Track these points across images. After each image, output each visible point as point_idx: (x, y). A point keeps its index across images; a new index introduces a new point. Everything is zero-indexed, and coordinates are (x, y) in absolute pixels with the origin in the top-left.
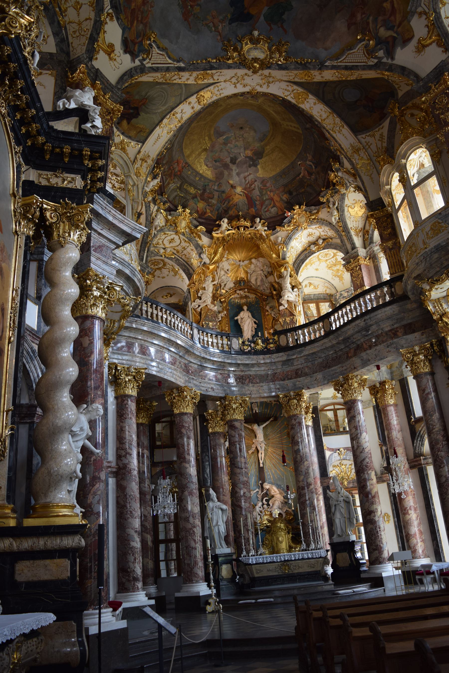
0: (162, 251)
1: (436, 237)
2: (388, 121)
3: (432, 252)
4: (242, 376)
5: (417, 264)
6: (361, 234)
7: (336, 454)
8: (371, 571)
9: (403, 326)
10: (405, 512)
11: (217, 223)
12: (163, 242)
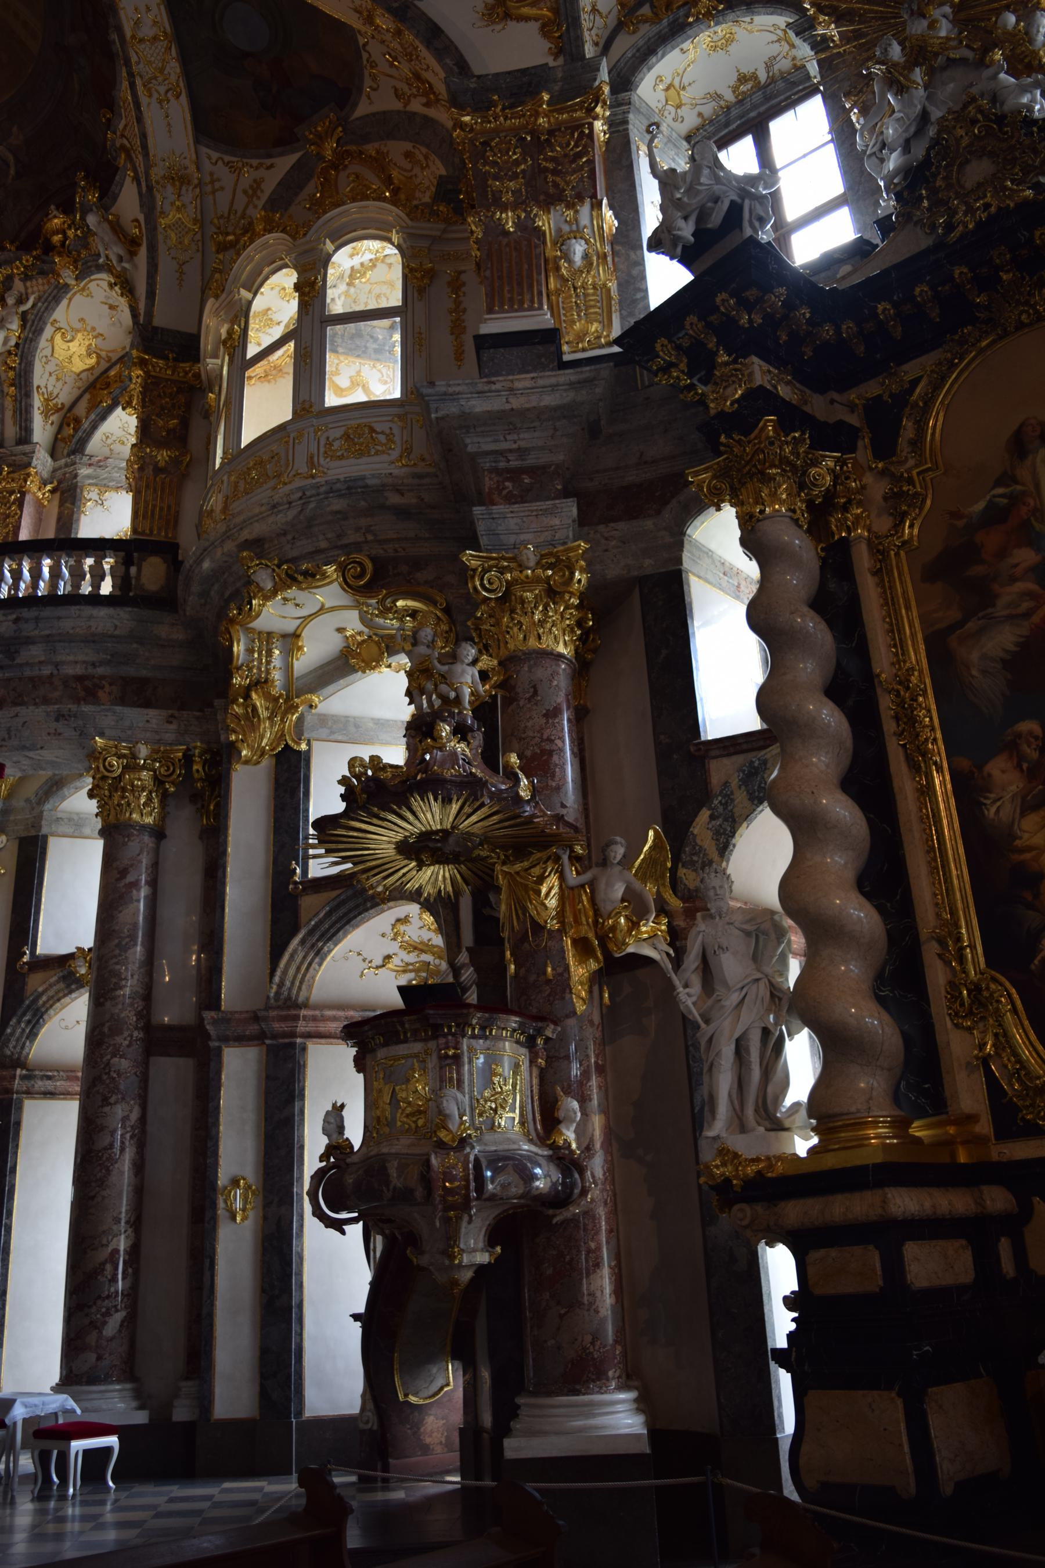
1: (352, 461)
2: (293, 159)
3: (332, 490)
5: (274, 507)
6: (54, 418)
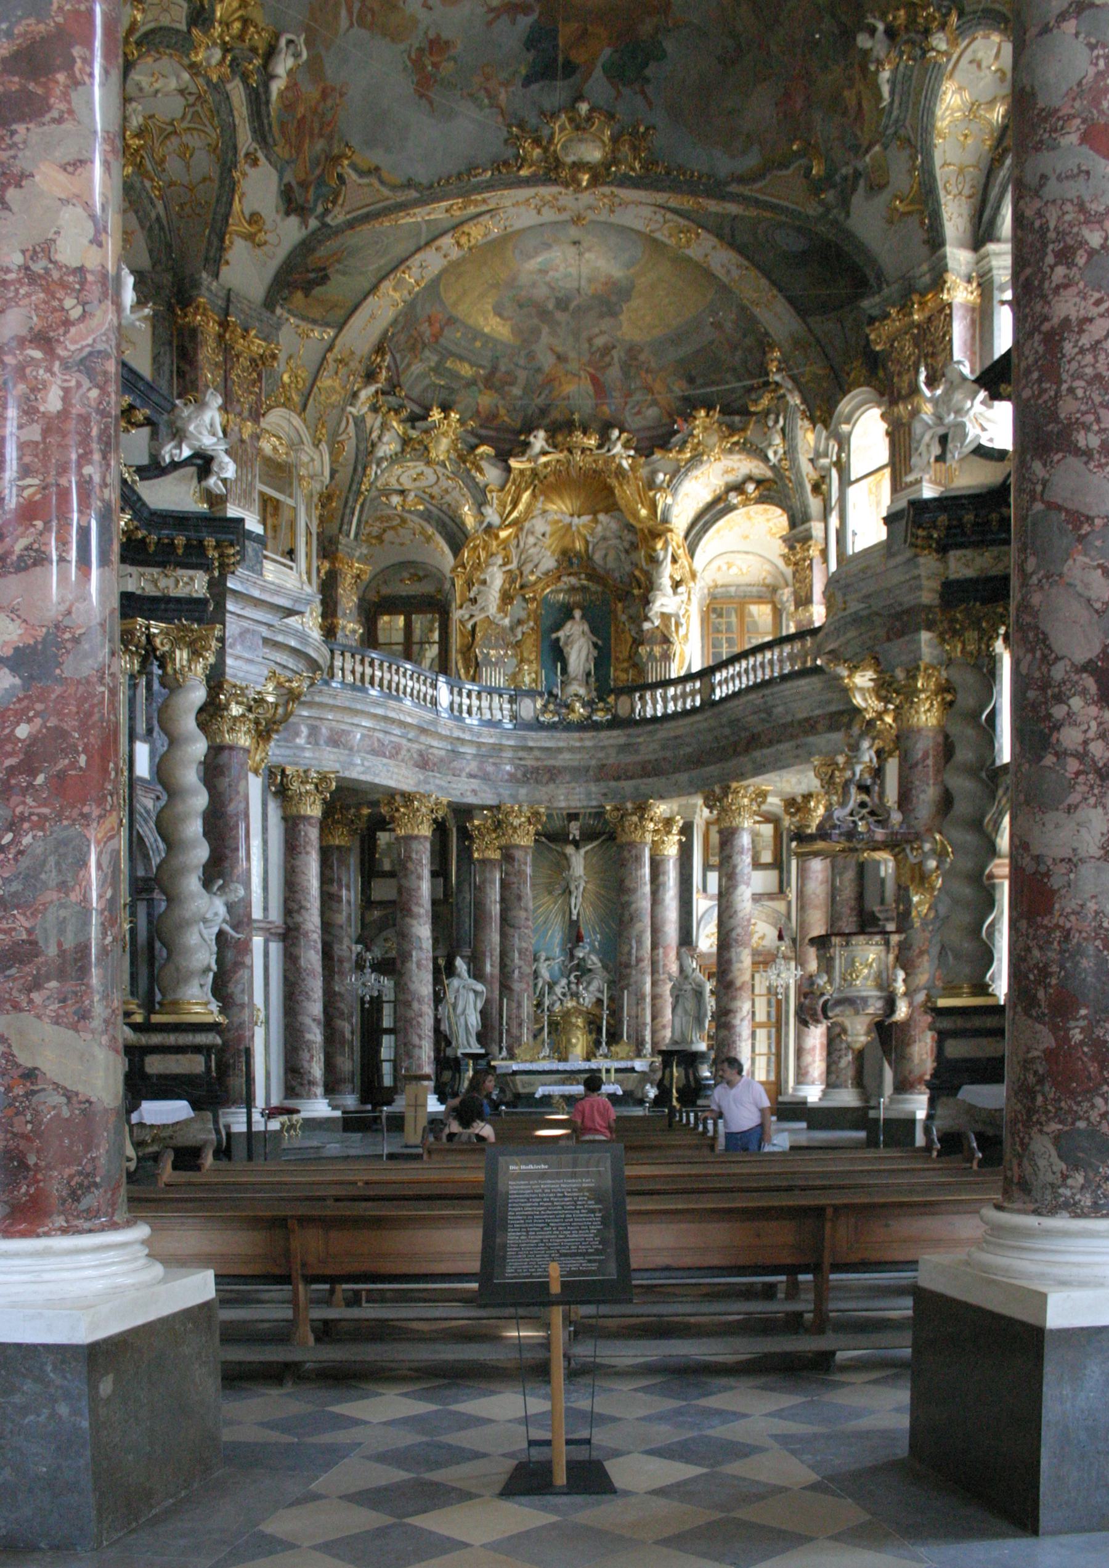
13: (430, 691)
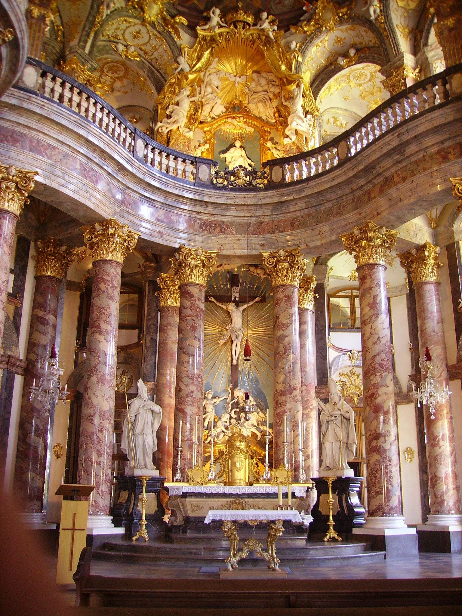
0: (121, 48)
4: (211, 223)
7: (346, 357)
8: (368, 526)
9: (458, 144)
10: (434, 441)
11: (205, 14)
12: (123, 34)
13: (129, 139)
